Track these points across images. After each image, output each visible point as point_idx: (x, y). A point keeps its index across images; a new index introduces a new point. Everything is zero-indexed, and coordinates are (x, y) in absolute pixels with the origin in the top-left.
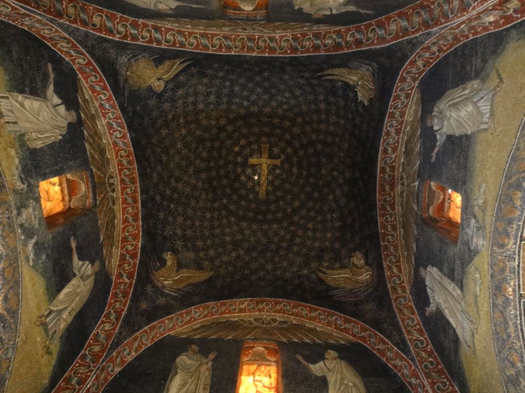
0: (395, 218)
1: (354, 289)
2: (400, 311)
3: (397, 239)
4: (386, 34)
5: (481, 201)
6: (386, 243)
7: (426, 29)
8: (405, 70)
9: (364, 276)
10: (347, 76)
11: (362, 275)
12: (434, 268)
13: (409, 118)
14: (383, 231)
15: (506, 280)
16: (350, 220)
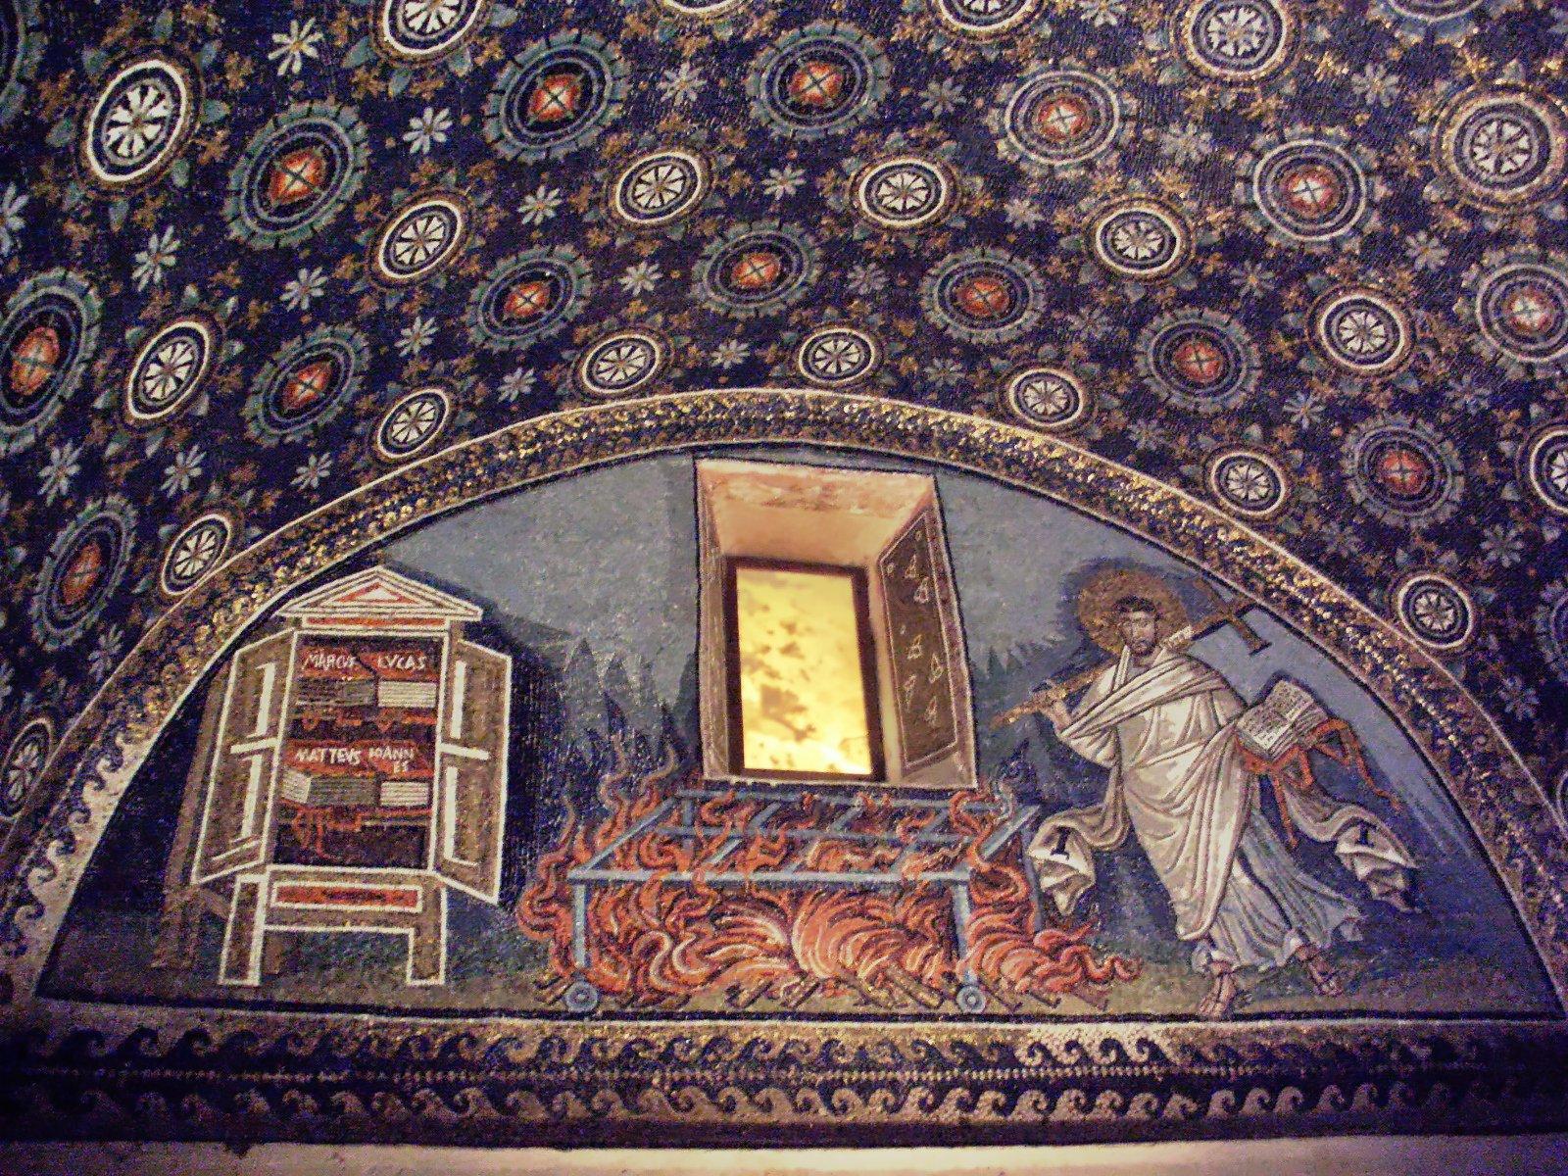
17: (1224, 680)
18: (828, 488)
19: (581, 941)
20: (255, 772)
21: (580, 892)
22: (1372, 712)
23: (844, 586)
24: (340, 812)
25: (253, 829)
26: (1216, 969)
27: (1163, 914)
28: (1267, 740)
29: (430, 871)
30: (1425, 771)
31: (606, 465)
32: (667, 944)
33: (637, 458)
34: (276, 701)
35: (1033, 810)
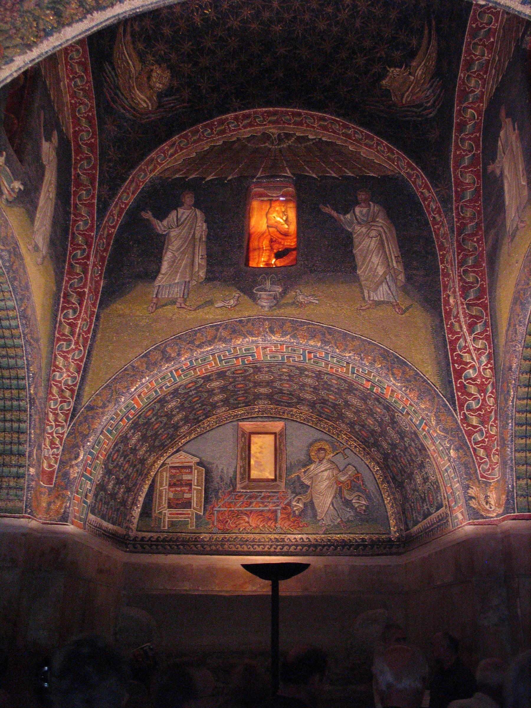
0: (234, 130)
1: (120, 91)
2: (132, 182)
3: (208, 138)
4: (464, 167)
5: (301, 298)
6: (201, 130)
7: (458, 228)
8: (422, 176)
9: (142, 96)
10: (424, 62)
11: (141, 92)
12: (205, 225)
13: (364, 152)
14: (216, 123)
15: (245, 338)
16: (209, 43)
17: (337, 466)
18: (264, 425)
19: (216, 521)
20: (164, 493)
21: (216, 512)
22: (368, 471)
23: (272, 437)
24: (178, 499)
25: (165, 504)
26: (323, 525)
27: (315, 515)
28: (343, 479)
29: (192, 509)
30: (376, 485)
31: (221, 425)
32: (229, 521)
33: (227, 423)
34: (166, 480)
35: (294, 495)
